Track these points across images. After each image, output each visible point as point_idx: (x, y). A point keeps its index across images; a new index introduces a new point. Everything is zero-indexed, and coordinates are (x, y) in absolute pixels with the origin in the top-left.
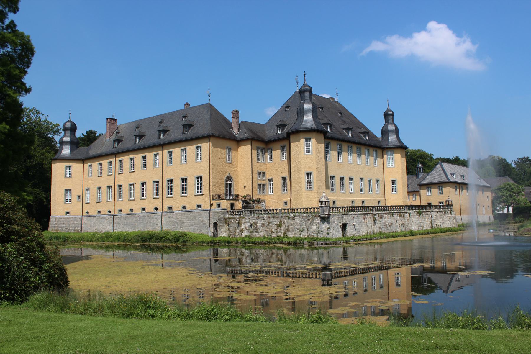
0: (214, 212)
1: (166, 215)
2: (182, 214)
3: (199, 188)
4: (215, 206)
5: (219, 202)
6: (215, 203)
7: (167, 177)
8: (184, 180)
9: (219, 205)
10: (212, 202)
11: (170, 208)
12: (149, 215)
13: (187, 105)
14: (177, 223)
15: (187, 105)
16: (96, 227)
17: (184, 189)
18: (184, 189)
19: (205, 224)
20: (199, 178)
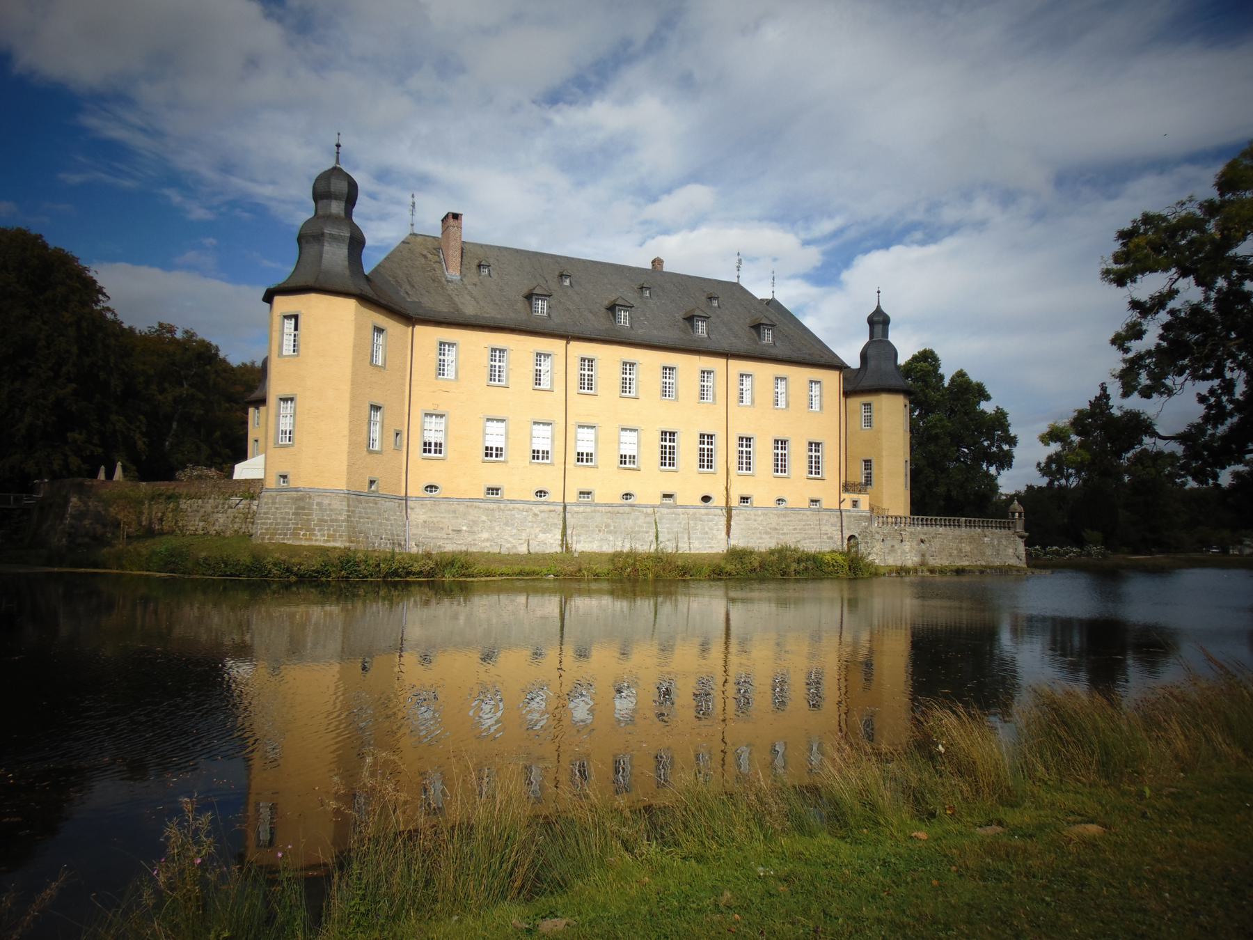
0: (849, 517)
1: (738, 515)
2: (779, 516)
3: (815, 467)
4: (847, 505)
5: (855, 496)
6: (848, 497)
7: (737, 430)
8: (781, 443)
9: (855, 504)
10: (844, 496)
11: (744, 499)
12: (691, 511)
13: (657, 262)
14: (767, 533)
15: (657, 262)
16: (485, 535)
17: (780, 464)
18: (780, 464)
19: (831, 538)
20: (815, 445)
